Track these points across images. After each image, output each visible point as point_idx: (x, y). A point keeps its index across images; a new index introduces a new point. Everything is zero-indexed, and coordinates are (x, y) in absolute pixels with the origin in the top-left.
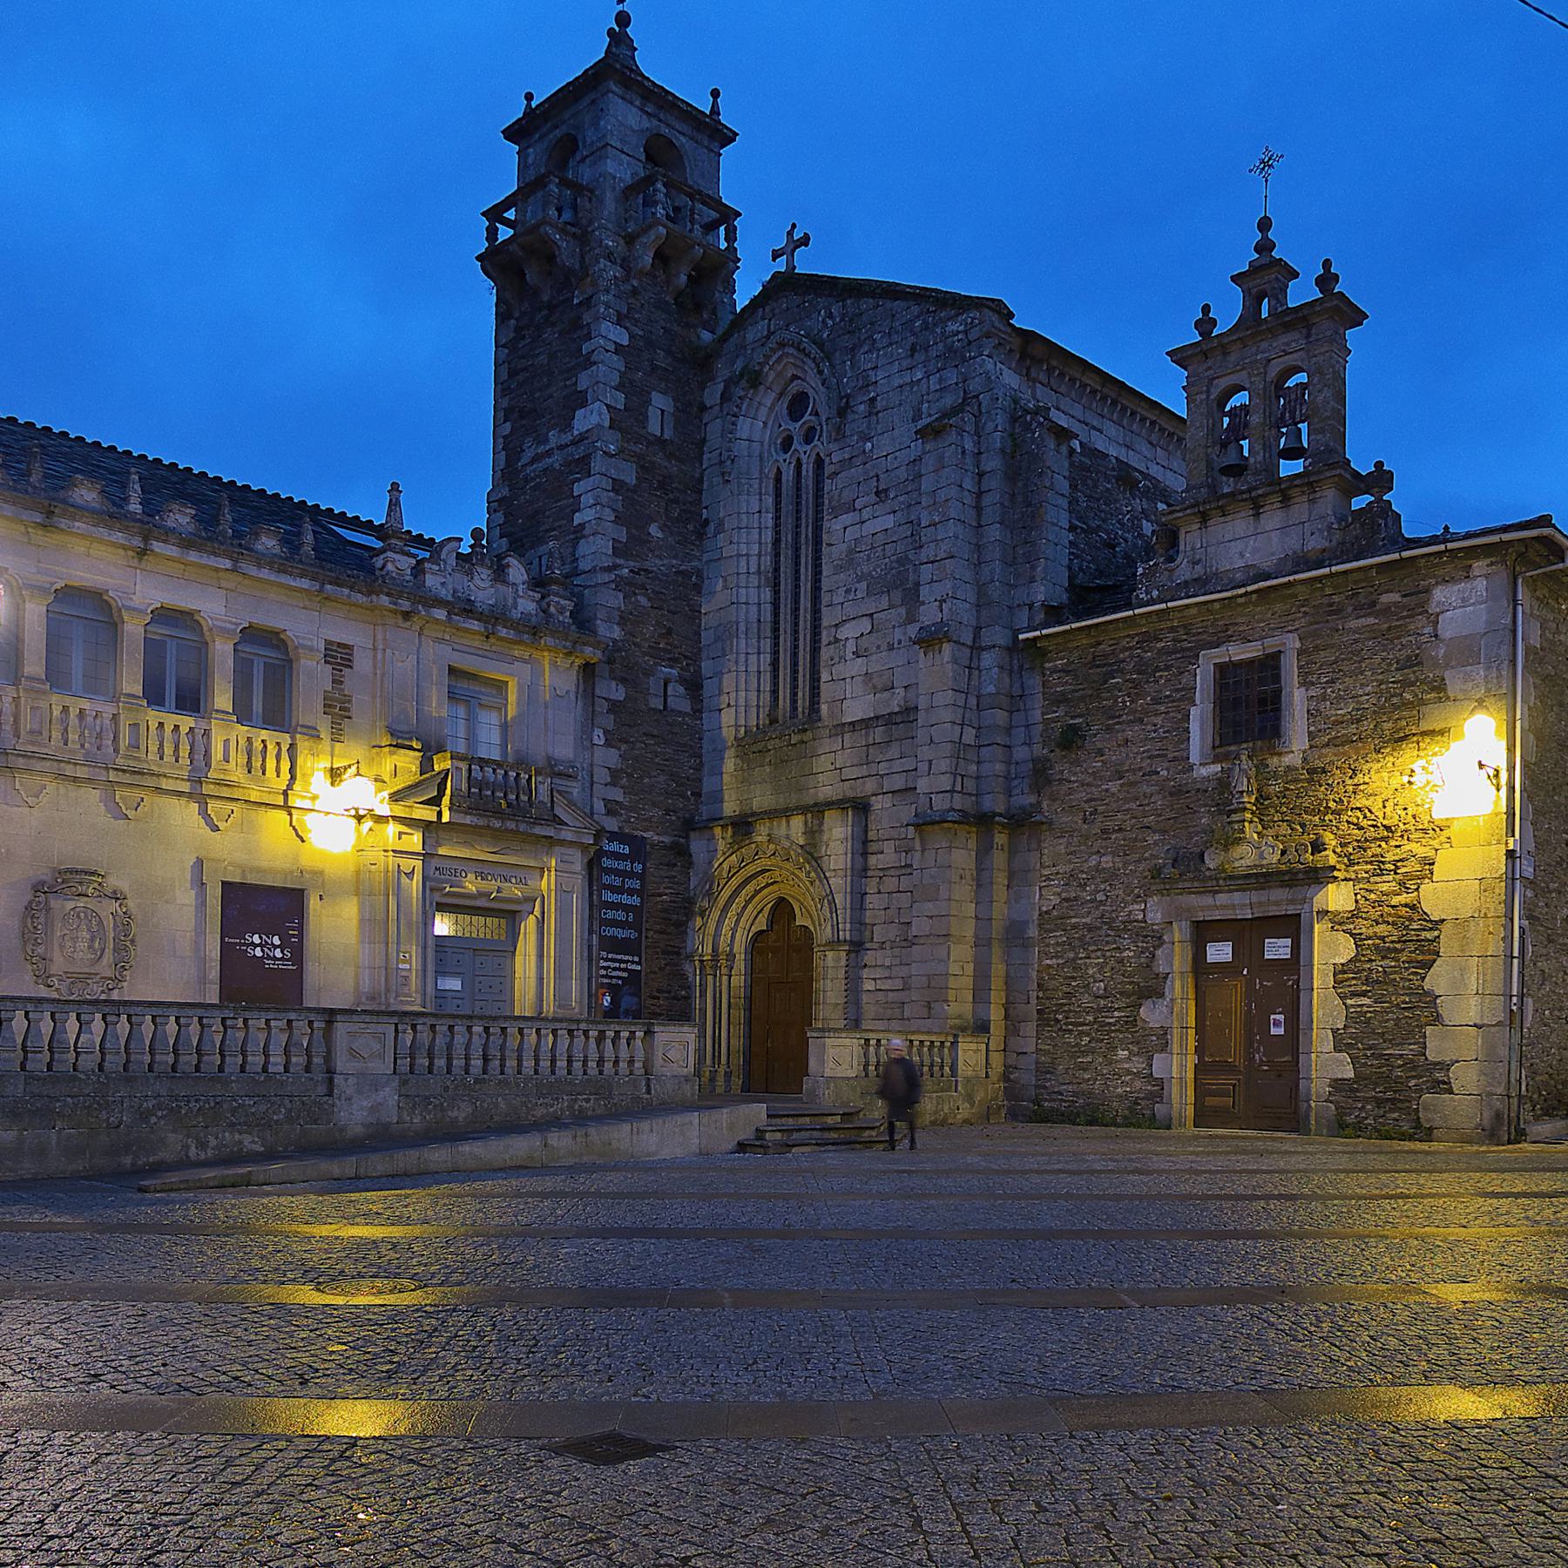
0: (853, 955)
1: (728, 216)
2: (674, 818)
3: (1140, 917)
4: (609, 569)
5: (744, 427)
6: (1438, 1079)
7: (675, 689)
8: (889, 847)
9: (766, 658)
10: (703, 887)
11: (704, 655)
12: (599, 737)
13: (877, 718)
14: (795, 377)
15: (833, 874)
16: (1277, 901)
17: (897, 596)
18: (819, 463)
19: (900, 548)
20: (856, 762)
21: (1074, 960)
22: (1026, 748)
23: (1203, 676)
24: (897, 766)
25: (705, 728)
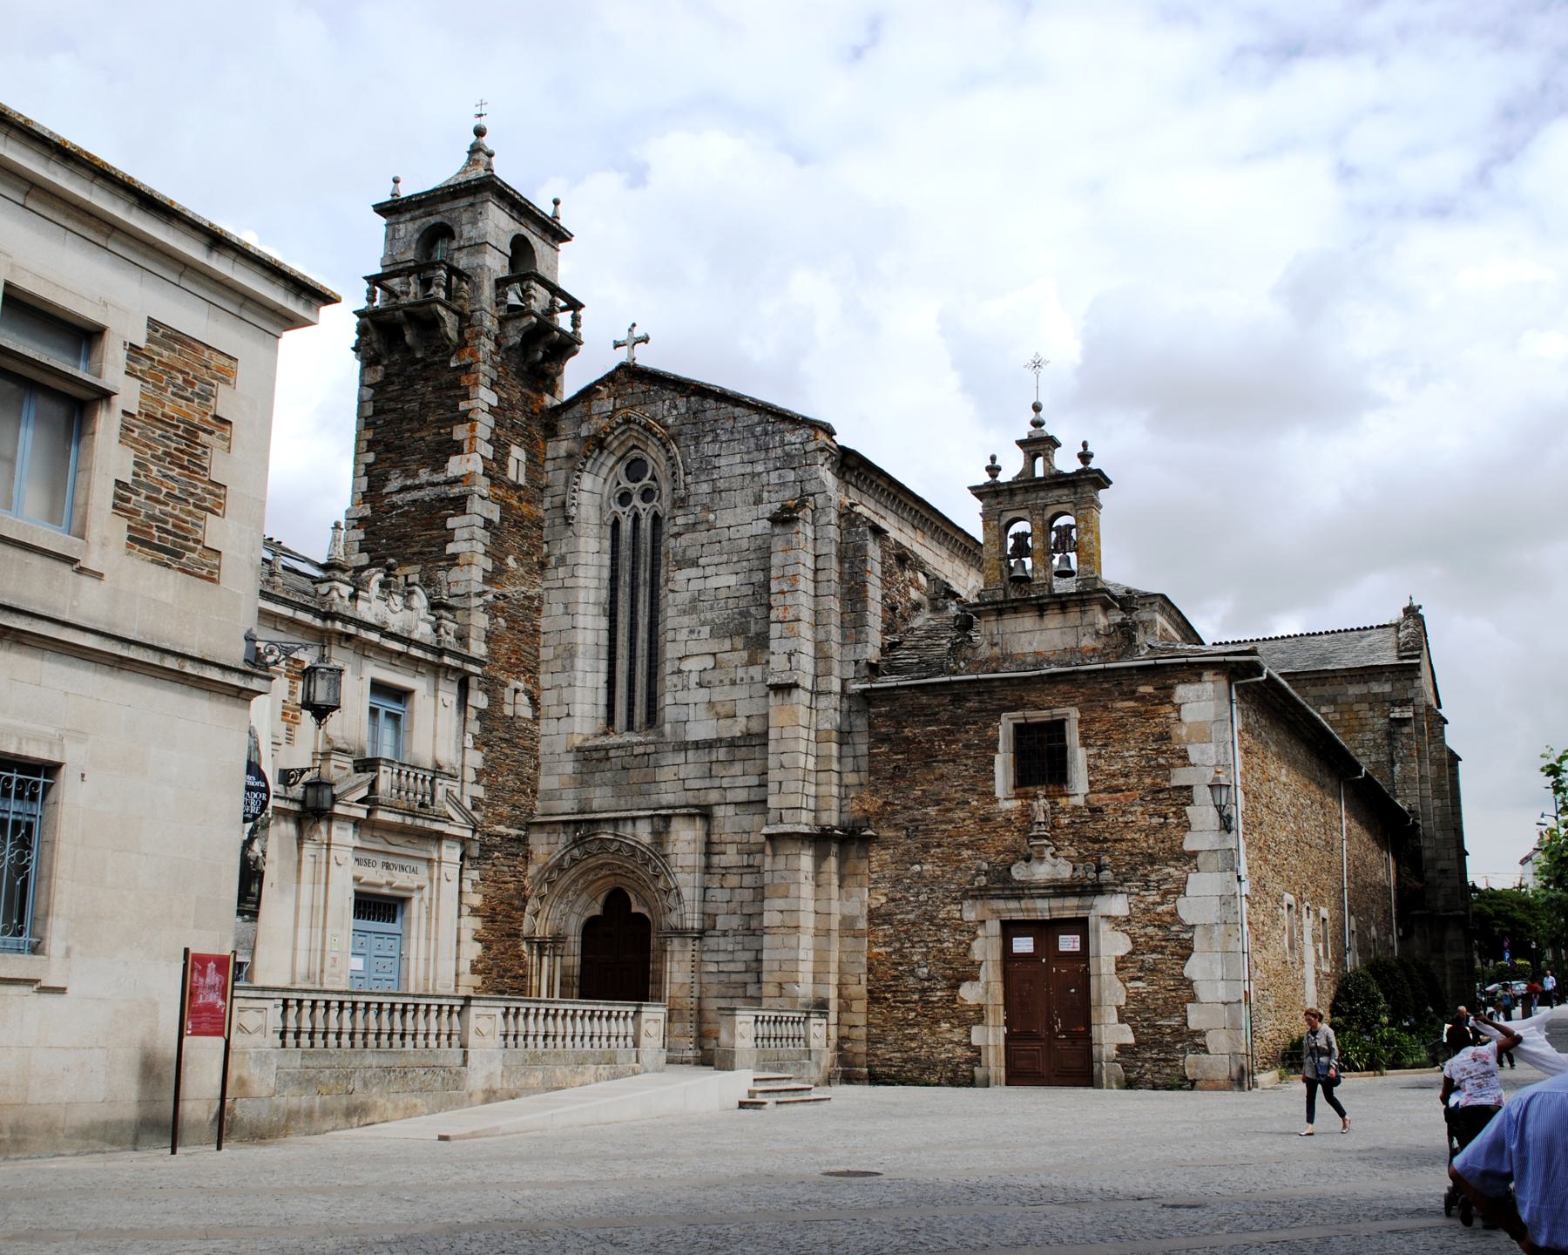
0: (697, 942)
1: (574, 305)
3: (958, 915)
4: (479, 595)
5: (587, 481)
6: (1195, 1041)
7: (523, 699)
8: (731, 850)
9: (603, 677)
11: (543, 668)
12: (469, 743)
13: (720, 740)
14: (634, 447)
16: (1068, 907)
17: (739, 642)
18: (657, 520)
19: (743, 603)
20: (699, 775)
21: (900, 949)
22: (855, 775)
23: (1004, 729)
24: (740, 782)
25: (542, 732)
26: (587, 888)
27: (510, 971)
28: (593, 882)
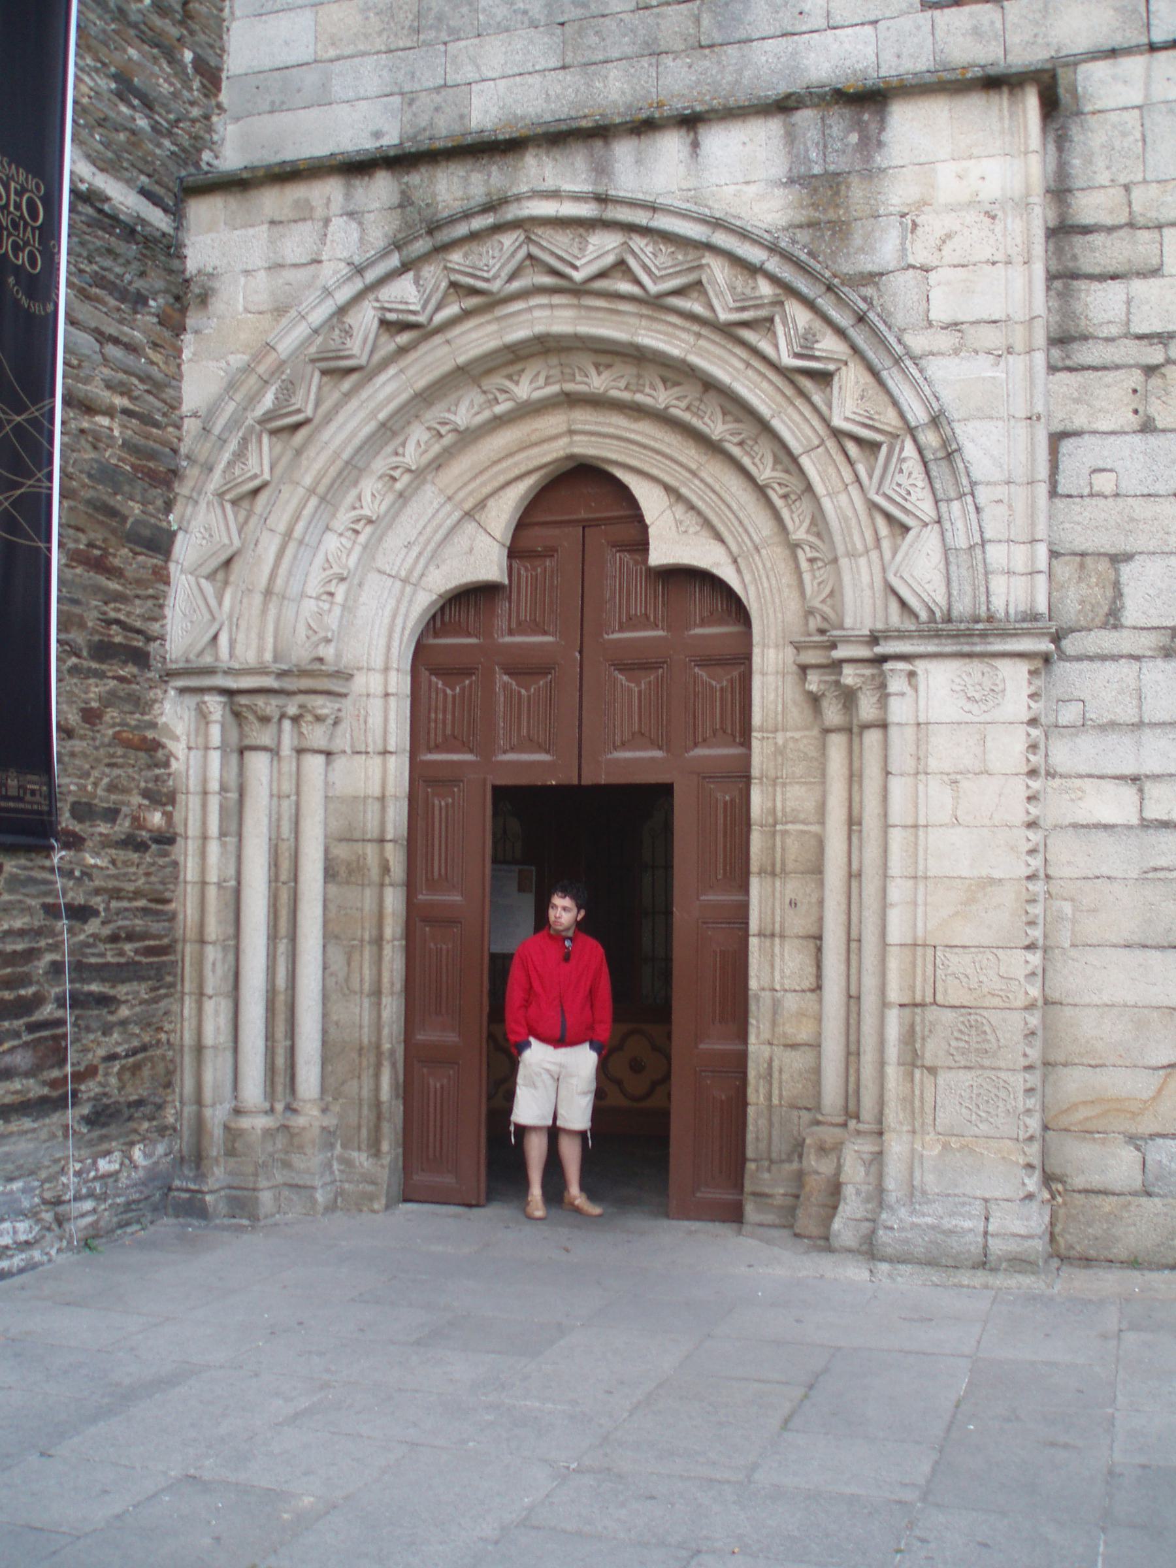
2: (142, 123)
10: (253, 399)
15: (945, 341)
26: (438, 464)
27: (112, 814)
28: (468, 437)
